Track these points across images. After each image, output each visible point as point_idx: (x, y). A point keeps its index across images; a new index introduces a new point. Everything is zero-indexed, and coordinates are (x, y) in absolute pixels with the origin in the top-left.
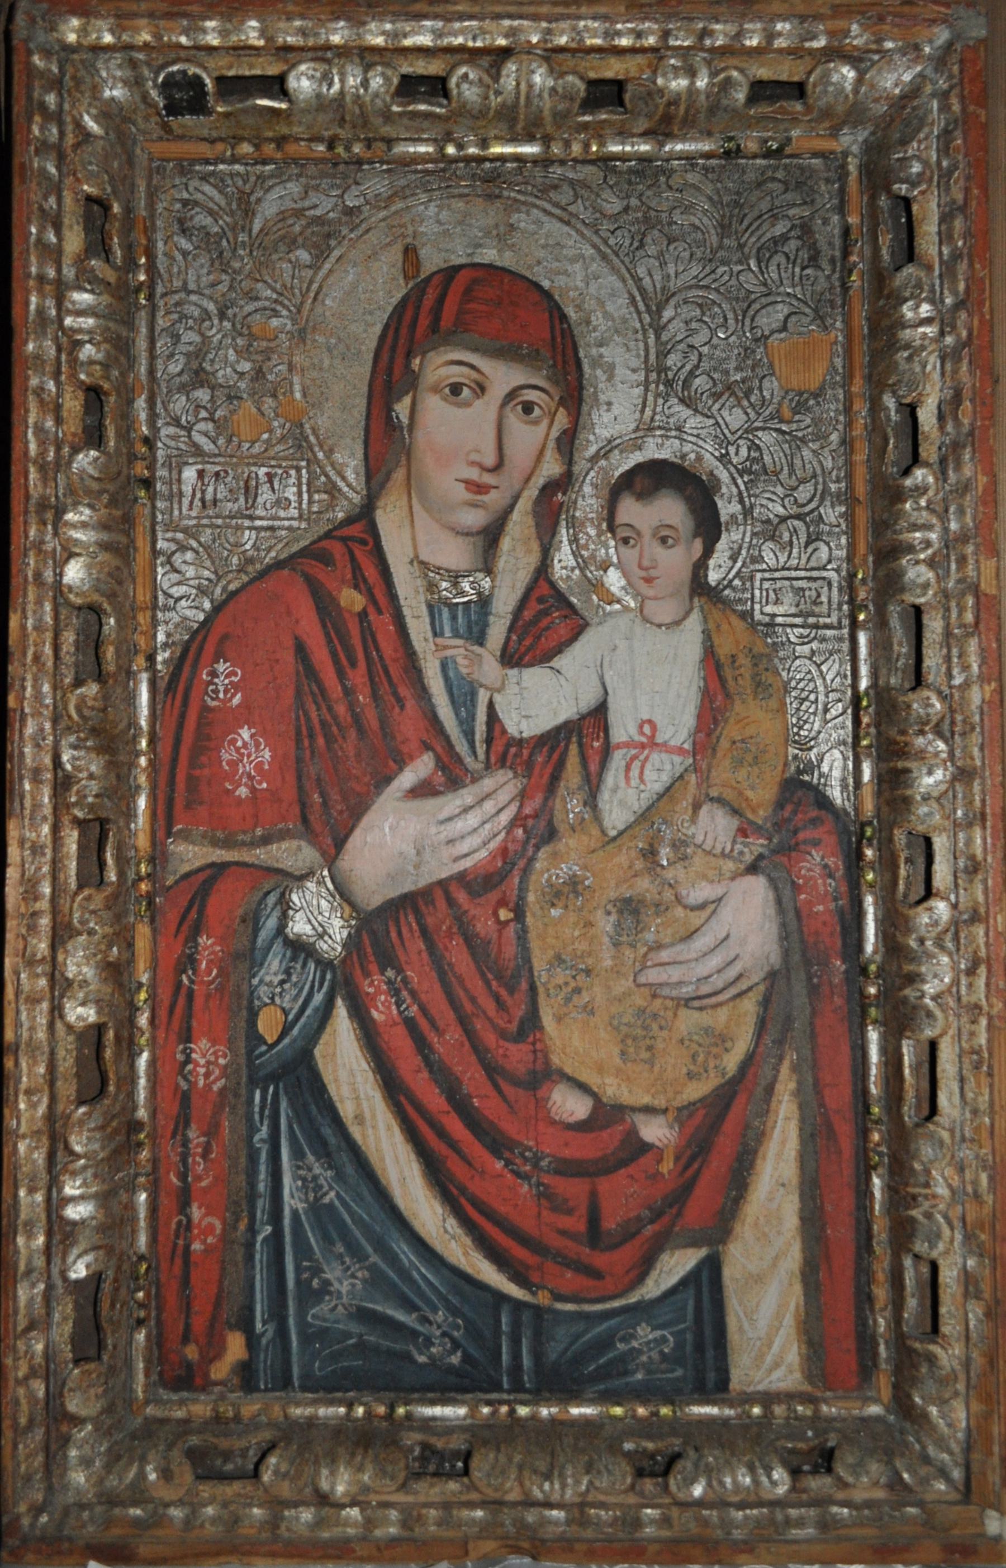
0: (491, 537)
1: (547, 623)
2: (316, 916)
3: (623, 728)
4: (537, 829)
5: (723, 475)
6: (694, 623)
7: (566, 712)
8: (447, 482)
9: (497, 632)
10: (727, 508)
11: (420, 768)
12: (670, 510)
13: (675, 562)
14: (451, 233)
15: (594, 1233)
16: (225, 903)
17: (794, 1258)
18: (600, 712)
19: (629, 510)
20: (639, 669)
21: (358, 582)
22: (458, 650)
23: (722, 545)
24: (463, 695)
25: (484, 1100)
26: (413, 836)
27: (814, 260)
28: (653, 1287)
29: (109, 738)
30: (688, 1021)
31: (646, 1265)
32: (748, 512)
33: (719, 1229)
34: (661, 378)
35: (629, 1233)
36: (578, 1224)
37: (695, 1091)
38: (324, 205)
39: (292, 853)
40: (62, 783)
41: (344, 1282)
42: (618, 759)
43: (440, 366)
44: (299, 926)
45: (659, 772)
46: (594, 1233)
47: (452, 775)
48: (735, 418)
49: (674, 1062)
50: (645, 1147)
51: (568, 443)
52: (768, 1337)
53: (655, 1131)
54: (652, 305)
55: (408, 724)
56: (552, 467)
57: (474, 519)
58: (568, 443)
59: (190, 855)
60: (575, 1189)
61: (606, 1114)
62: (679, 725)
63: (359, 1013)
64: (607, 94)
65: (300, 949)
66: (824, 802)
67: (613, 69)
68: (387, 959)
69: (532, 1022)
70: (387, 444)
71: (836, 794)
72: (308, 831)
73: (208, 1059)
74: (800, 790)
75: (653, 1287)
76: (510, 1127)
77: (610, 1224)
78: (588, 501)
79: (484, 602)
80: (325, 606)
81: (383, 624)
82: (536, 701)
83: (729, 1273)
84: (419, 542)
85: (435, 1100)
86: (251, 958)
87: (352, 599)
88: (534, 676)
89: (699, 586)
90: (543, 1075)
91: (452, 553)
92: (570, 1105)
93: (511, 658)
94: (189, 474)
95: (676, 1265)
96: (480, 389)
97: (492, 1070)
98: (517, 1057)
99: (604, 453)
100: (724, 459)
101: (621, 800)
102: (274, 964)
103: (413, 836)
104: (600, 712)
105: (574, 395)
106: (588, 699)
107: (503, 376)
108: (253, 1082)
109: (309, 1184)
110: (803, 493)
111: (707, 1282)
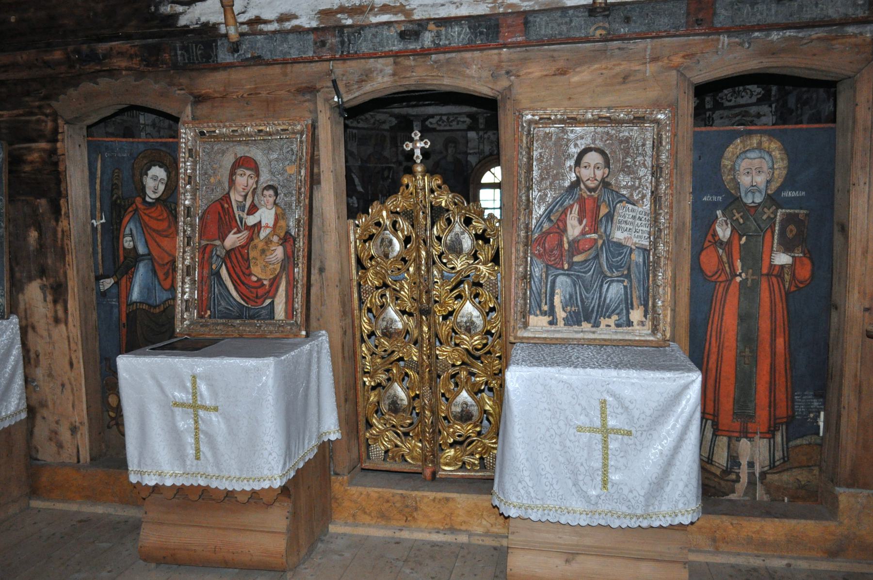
0: (245, 197)
1: (253, 209)
3: (263, 224)
4: (251, 239)
6: (273, 211)
7: (256, 222)
8: (240, 189)
10: (279, 192)
11: (235, 230)
12: (271, 192)
13: (272, 200)
15: (257, 297)
16: (208, 250)
17: (284, 300)
18: (260, 222)
19: (265, 192)
20: (266, 216)
21: (227, 203)
22: (241, 213)
24: (241, 220)
25: (243, 278)
26: (232, 240)
28: (265, 305)
29: (192, 226)
30: (271, 267)
31: (264, 301)
33: (274, 297)
35: (262, 296)
36: (255, 295)
37: (272, 277)
39: (218, 243)
40: (185, 231)
41: (223, 303)
43: (239, 171)
44: (218, 253)
45: (268, 231)
46: (257, 297)
47: (239, 231)
49: (269, 273)
50: (263, 285)
51: (257, 182)
52: (280, 311)
53: (265, 282)
55: (234, 224)
56: (255, 186)
57: (243, 194)
58: (257, 182)
59: (204, 243)
60: (254, 291)
61: (259, 280)
62: (271, 224)
63: (226, 265)
64: (260, 131)
65: (218, 256)
66: (291, 235)
67: (261, 128)
68: (230, 258)
69: (249, 267)
70: (232, 182)
72: (219, 239)
73: (206, 272)
74: (288, 233)
75: (265, 305)
76: (245, 281)
77: (259, 295)
78: (259, 191)
79: (244, 206)
80: (222, 207)
81: (230, 209)
82: (251, 220)
83: (275, 303)
84: (236, 197)
85: (236, 278)
86: (212, 257)
87: (226, 206)
88: (251, 217)
89: (275, 203)
90: (251, 274)
91: (240, 199)
92: (254, 279)
93: (248, 214)
95: (268, 301)
97: (244, 273)
98: (247, 272)
101: (263, 234)
102: (215, 258)
103: (232, 240)
104: (260, 222)
105: (258, 175)
106: (258, 220)
107: (248, 173)
108: (212, 275)
109: (219, 290)
111: (272, 304)
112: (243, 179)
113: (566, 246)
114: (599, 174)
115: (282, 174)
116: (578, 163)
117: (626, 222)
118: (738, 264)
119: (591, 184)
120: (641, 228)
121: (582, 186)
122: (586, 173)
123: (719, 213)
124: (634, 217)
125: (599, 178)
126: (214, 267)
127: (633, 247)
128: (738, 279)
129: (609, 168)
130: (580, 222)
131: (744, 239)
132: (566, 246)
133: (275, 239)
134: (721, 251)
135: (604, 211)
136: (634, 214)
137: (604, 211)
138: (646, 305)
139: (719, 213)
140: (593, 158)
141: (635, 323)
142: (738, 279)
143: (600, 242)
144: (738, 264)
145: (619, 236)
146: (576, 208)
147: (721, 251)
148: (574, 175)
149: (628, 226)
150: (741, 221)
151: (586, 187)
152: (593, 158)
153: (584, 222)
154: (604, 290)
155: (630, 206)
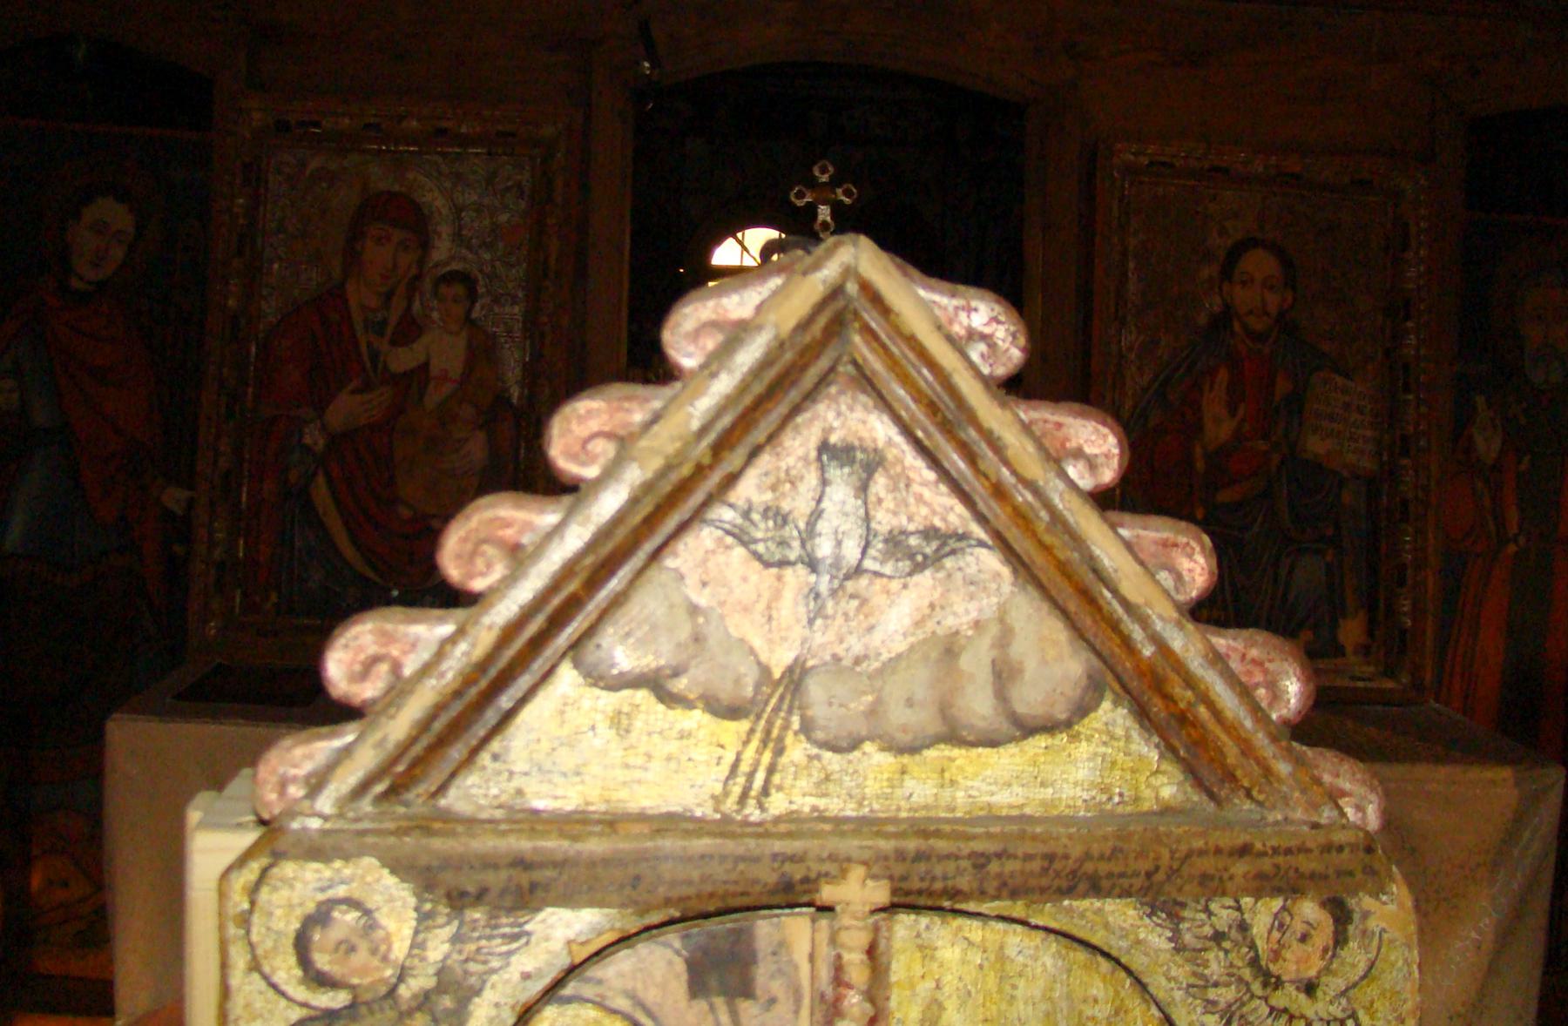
0: (389, 296)
1: (410, 330)
2: (314, 438)
3: (435, 370)
5: (480, 277)
6: (464, 334)
7: (413, 364)
9: (389, 330)
10: (481, 290)
12: (459, 289)
14: (381, 179)
19: (443, 289)
20: (443, 351)
23: (478, 306)
24: (375, 356)
27: (521, 196)
32: (488, 292)
34: (457, 236)
38: (333, 166)
42: (432, 386)
44: (308, 440)
45: (448, 388)
47: (367, 387)
48: (487, 256)
54: (458, 210)
56: (414, 271)
57: (383, 289)
58: (421, 262)
65: (308, 450)
66: (511, 405)
67: (444, 124)
71: (515, 401)
74: (501, 399)
78: (427, 284)
79: (385, 322)
82: (403, 359)
84: (360, 297)
92: (405, 512)
93: (394, 343)
94: (276, 266)
96: (388, 239)
99: (436, 266)
100: (481, 271)
105: (425, 245)
106: (422, 358)
107: (398, 235)
110: (510, 285)
112: (380, 254)
113: (1200, 465)
114: (1273, 301)
115: (489, 246)
116: (1227, 272)
117: (1331, 418)
118: (1513, 515)
119: (1257, 324)
120: (1360, 432)
121: (1237, 326)
122: (1243, 297)
123: (1480, 400)
124: (1347, 406)
125: (1273, 309)
126: (293, 476)
127: (1345, 474)
128: (1512, 548)
129: (1294, 288)
130: (1233, 411)
131: (1526, 459)
132: (1200, 465)
133: (467, 411)
134: (1479, 485)
135: (1282, 387)
136: (1347, 399)
137: (1282, 387)
138: (1371, 608)
139: (1480, 400)
140: (1259, 264)
141: (1349, 650)
142: (1512, 548)
143: (1276, 458)
144: (1513, 515)
145: (1315, 445)
146: (1223, 376)
147: (1479, 485)
148: (1218, 300)
149: (1335, 425)
150: (1523, 421)
151: (1245, 327)
152: (1259, 264)
153: (1241, 411)
154: (1283, 572)
155: (1339, 380)
